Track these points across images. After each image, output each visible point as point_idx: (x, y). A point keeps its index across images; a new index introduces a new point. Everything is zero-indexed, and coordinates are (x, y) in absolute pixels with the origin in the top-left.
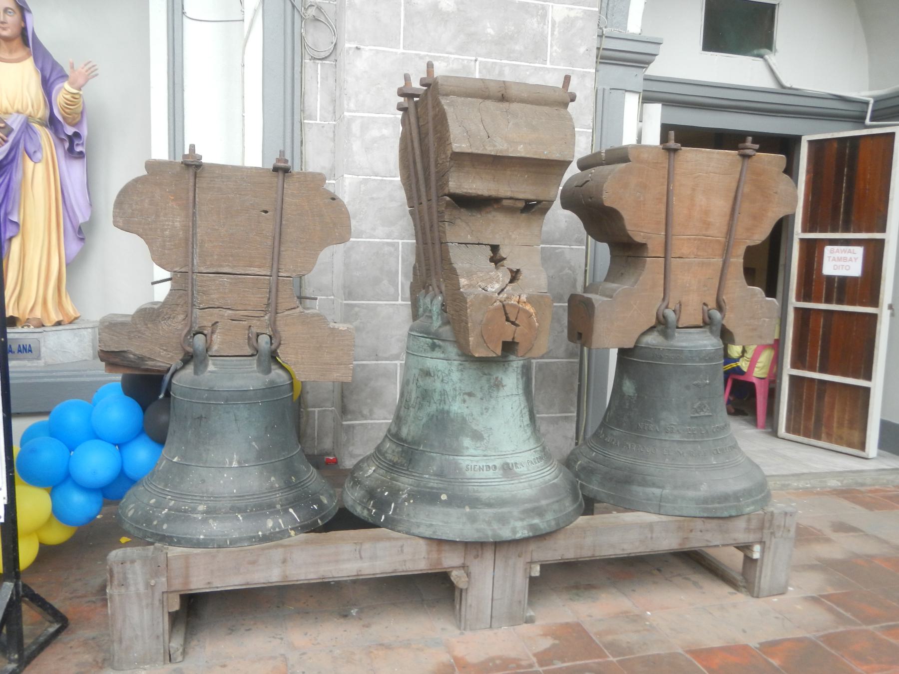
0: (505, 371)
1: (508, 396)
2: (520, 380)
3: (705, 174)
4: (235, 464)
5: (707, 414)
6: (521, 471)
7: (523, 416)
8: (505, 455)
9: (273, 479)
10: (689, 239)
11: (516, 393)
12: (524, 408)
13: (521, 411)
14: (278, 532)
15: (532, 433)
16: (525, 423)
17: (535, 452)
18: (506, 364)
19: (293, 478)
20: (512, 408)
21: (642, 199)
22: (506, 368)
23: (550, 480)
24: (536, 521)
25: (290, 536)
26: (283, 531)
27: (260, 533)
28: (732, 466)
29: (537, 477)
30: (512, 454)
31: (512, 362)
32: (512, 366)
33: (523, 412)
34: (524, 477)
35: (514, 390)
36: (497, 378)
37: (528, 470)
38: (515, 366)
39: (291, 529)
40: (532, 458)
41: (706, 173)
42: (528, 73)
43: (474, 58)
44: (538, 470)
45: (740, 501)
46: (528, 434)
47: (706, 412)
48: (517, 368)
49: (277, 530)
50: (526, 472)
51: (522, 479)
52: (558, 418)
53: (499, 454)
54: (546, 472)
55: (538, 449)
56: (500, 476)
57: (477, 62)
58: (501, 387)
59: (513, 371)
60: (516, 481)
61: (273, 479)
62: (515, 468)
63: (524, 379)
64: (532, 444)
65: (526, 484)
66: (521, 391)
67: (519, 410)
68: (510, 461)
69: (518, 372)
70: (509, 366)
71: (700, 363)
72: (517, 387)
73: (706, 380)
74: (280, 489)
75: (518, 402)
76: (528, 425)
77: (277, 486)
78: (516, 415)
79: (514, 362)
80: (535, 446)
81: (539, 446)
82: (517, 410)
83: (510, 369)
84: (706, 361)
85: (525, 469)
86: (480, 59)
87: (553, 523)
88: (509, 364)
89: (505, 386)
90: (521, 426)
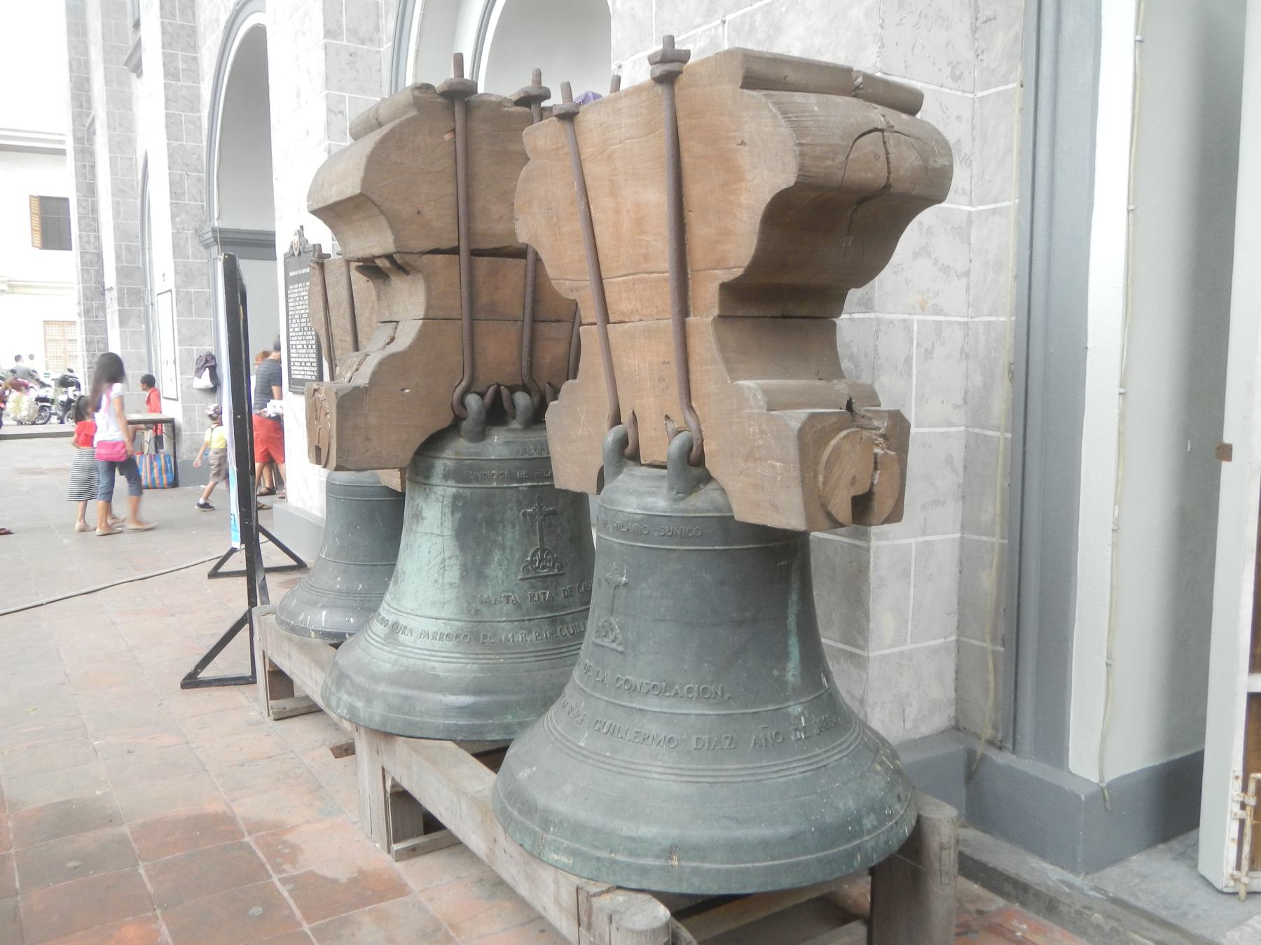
0: (426, 498)
1: (426, 534)
2: (449, 515)
3: (618, 146)
4: (323, 557)
5: (614, 645)
6: (404, 640)
7: (446, 568)
8: (400, 611)
9: (339, 579)
10: (625, 282)
11: (436, 531)
12: (450, 558)
13: (444, 561)
14: (303, 628)
15: (457, 598)
16: (447, 580)
17: (445, 624)
18: (427, 487)
19: (360, 586)
20: (429, 552)
21: (555, 220)
22: (427, 494)
23: (433, 668)
24: (360, 704)
25: (310, 637)
26: (306, 628)
27: (292, 622)
28: (608, 767)
29: (417, 656)
30: (407, 613)
31: (435, 487)
32: (435, 493)
33: (447, 562)
34: (401, 648)
35: (436, 527)
36: (418, 505)
37: (415, 642)
38: (439, 493)
39: (313, 630)
40: (431, 630)
41: (620, 143)
42: (783, 9)
43: (719, 22)
44: (431, 648)
45: (546, 831)
46: (445, 596)
47: (613, 642)
48: (443, 497)
49: (303, 625)
50: (408, 644)
51: (396, 649)
52: (839, 650)
53: (398, 608)
54: (440, 657)
55: (457, 623)
56: (383, 636)
57: (726, 24)
58: (420, 519)
59: (436, 499)
60: (389, 649)
61: (339, 579)
62: (401, 632)
63: (458, 515)
64: (449, 611)
65: (394, 657)
66: (448, 532)
67: (439, 559)
68: (403, 622)
69: (445, 503)
70: (430, 491)
71: (613, 537)
72: (441, 525)
73: (622, 576)
74: (339, 591)
75: (440, 546)
76: (451, 584)
77: (338, 586)
78: (433, 562)
79: (438, 488)
80: (452, 616)
81: (466, 621)
82: (436, 557)
83: (433, 496)
84: (624, 535)
85: (412, 639)
86: (728, 18)
87: (377, 718)
88: (430, 488)
89: (425, 518)
90: (436, 581)
